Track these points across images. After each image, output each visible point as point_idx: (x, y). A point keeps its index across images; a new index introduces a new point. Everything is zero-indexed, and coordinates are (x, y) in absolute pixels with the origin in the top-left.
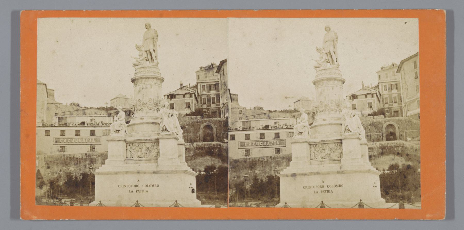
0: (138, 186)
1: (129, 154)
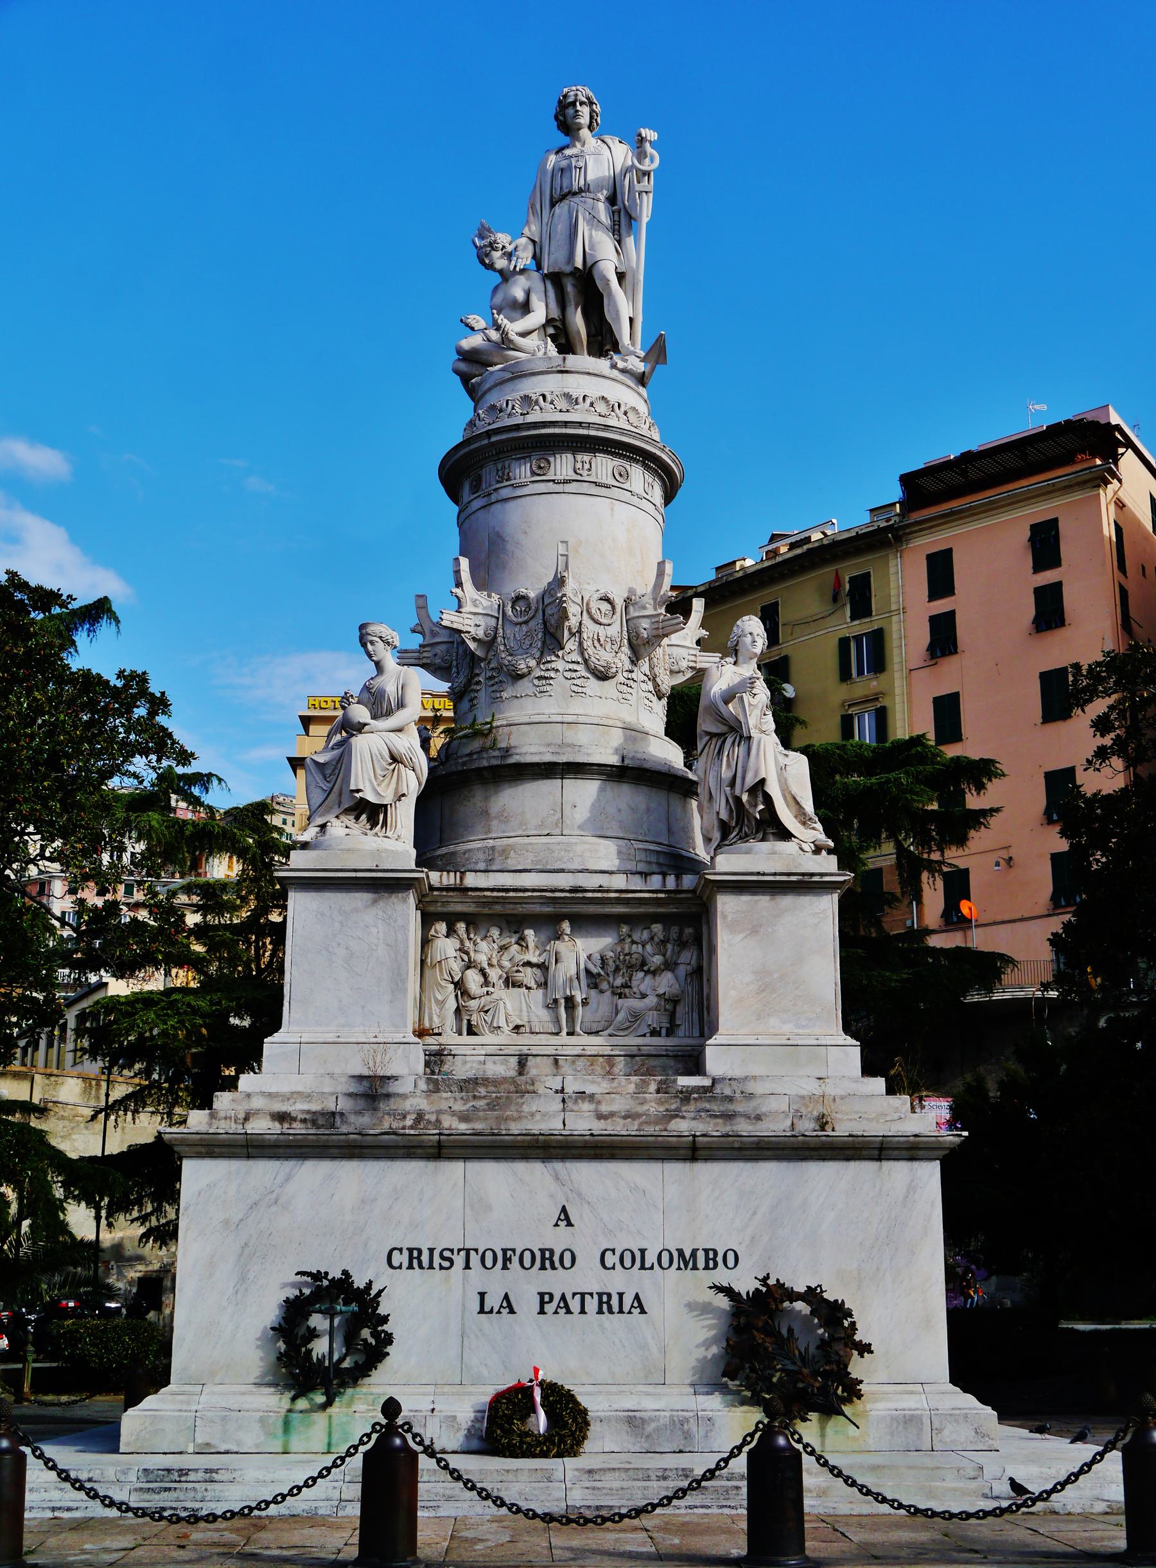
0: (567, 1263)
1: (441, 1004)
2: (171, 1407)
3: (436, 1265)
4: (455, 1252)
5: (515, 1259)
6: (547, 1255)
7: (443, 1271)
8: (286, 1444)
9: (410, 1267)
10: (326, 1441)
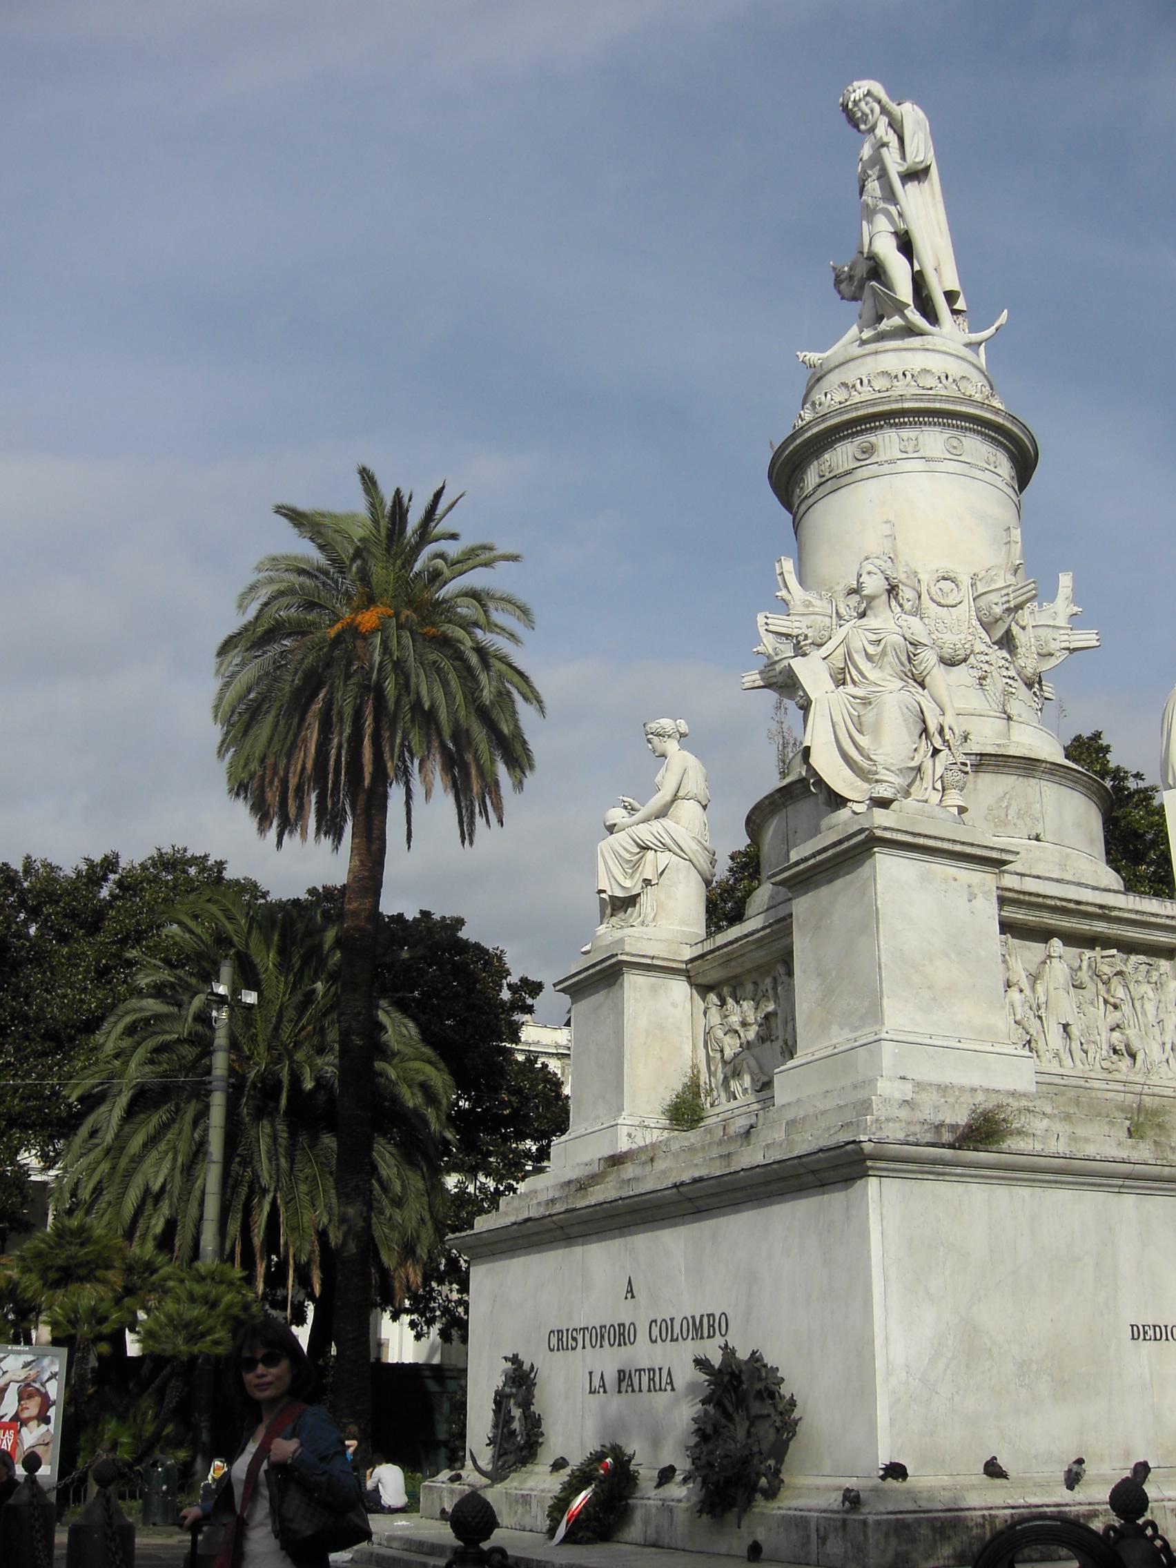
0: (632, 1340)
9: (558, 1350)
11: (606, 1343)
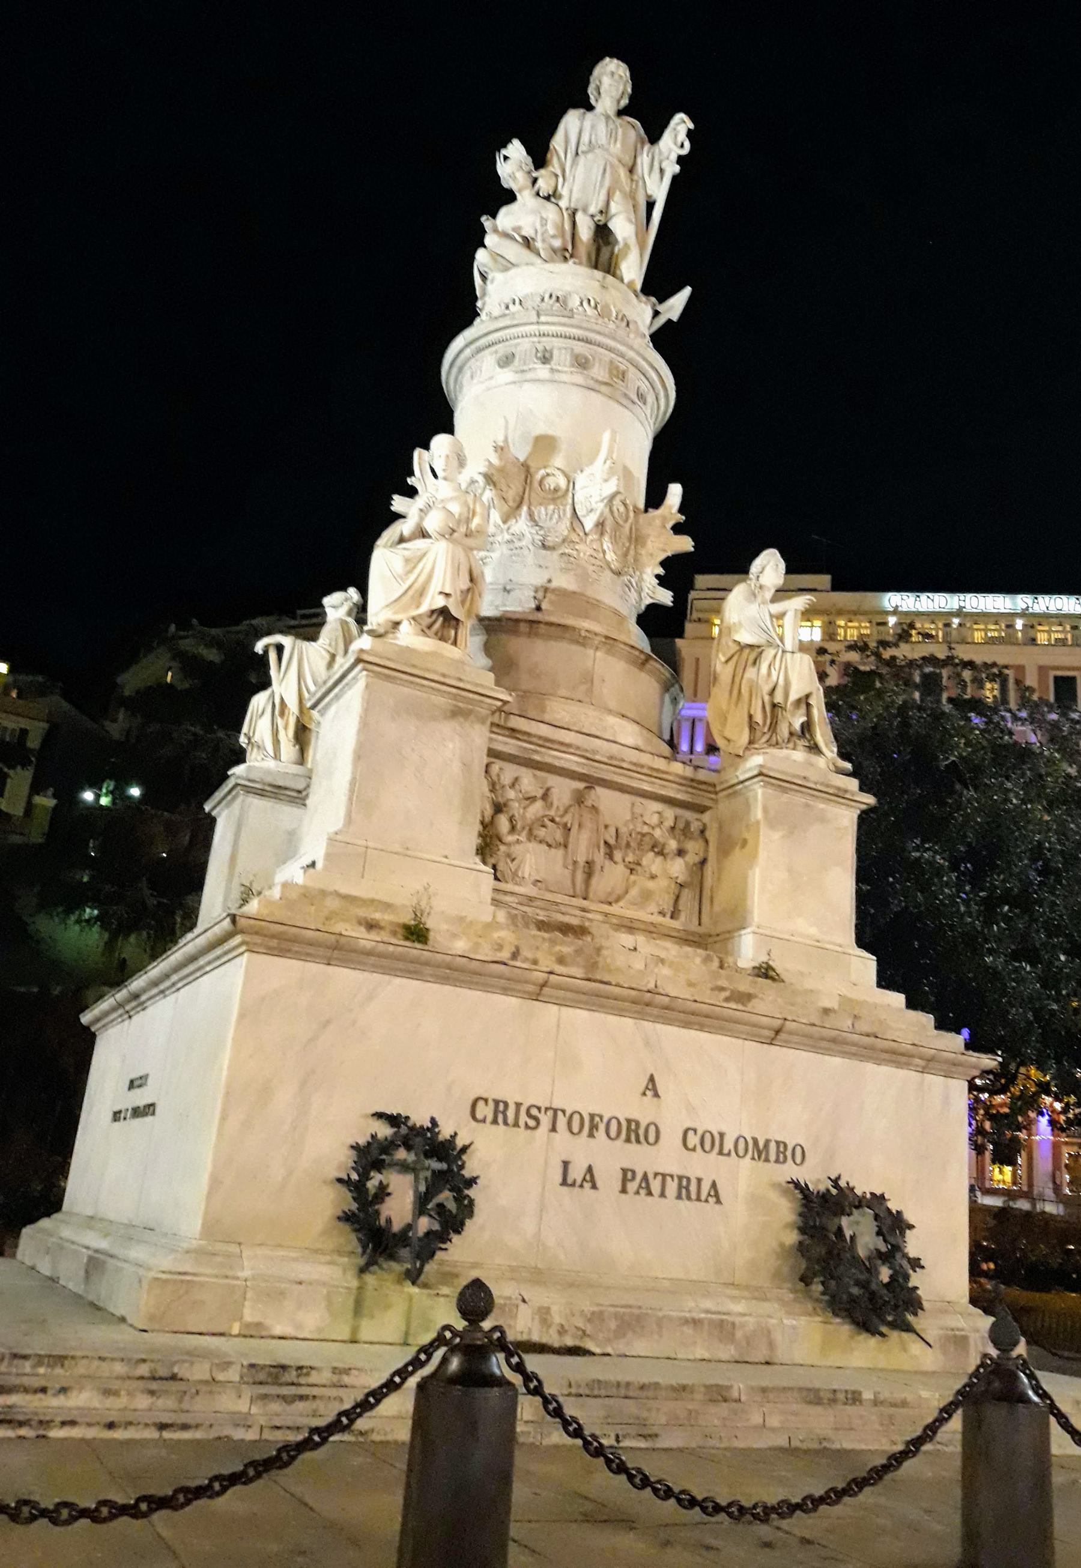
0: (652, 1139)
2: (208, 1271)
3: (522, 1123)
4: (543, 1110)
5: (602, 1127)
6: (633, 1127)
7: (529, 1131)
8: (355, 1330)
9: (495, 1122)
10: (403, 1328)
11: (601, 1133)
